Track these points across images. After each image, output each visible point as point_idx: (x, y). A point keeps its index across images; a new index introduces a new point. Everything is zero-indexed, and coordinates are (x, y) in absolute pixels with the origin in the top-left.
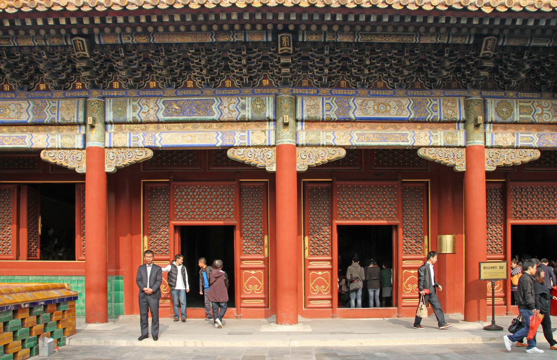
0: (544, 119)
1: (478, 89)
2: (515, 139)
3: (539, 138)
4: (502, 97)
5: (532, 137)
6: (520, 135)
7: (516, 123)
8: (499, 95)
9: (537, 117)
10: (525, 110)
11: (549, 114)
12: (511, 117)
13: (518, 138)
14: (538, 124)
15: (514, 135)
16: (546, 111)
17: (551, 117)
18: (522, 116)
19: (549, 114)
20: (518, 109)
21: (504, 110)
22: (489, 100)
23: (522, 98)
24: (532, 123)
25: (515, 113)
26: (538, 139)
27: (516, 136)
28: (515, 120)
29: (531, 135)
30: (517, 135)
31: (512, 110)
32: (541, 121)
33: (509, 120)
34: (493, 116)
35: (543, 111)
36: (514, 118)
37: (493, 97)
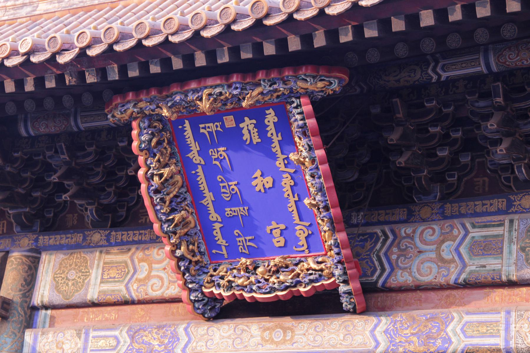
0: (150, 291)
1: (34, 232)
2: (80, 344)
3: (132, 338)
4: (78, 246)
5: (116, 338)
6: (92, 334)
7: (94, 305)
8: (73, 242)
9: (135, 286)
10: (113, 273)
11: (161, 279)
12: (82, 292)
13: (86, 341)
14: (140, 302)
15: (79, 335)
16: (158, 270)
17: (166, 283)
18: (105, 287)
19: (161, 279)
20: (100, 271)
21: (72, 275)
22: (45, 257)
23: (117, 244)
24: (126, 303)
25: (92, 282)
26: (128, 340)
27: (83, 336)
28: (89, 297)
29: (117, 333)
30: (87, 334)
31: (87, 275)
32: (142, 296)
33: (76, 299)
34: (46, 293)
35: (151, 269)
36: (86, 295)
37: (58, 248)
